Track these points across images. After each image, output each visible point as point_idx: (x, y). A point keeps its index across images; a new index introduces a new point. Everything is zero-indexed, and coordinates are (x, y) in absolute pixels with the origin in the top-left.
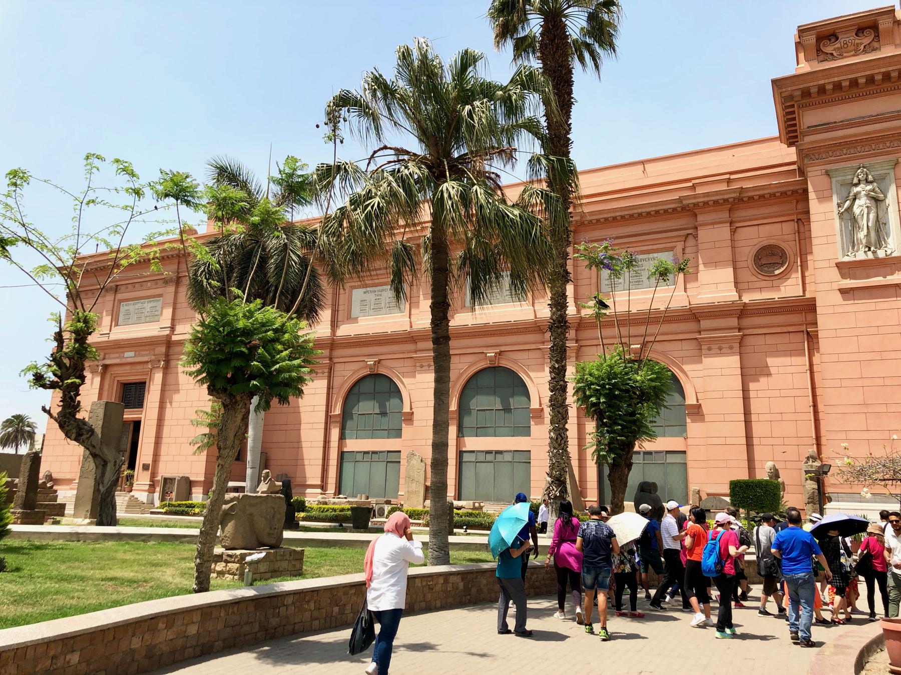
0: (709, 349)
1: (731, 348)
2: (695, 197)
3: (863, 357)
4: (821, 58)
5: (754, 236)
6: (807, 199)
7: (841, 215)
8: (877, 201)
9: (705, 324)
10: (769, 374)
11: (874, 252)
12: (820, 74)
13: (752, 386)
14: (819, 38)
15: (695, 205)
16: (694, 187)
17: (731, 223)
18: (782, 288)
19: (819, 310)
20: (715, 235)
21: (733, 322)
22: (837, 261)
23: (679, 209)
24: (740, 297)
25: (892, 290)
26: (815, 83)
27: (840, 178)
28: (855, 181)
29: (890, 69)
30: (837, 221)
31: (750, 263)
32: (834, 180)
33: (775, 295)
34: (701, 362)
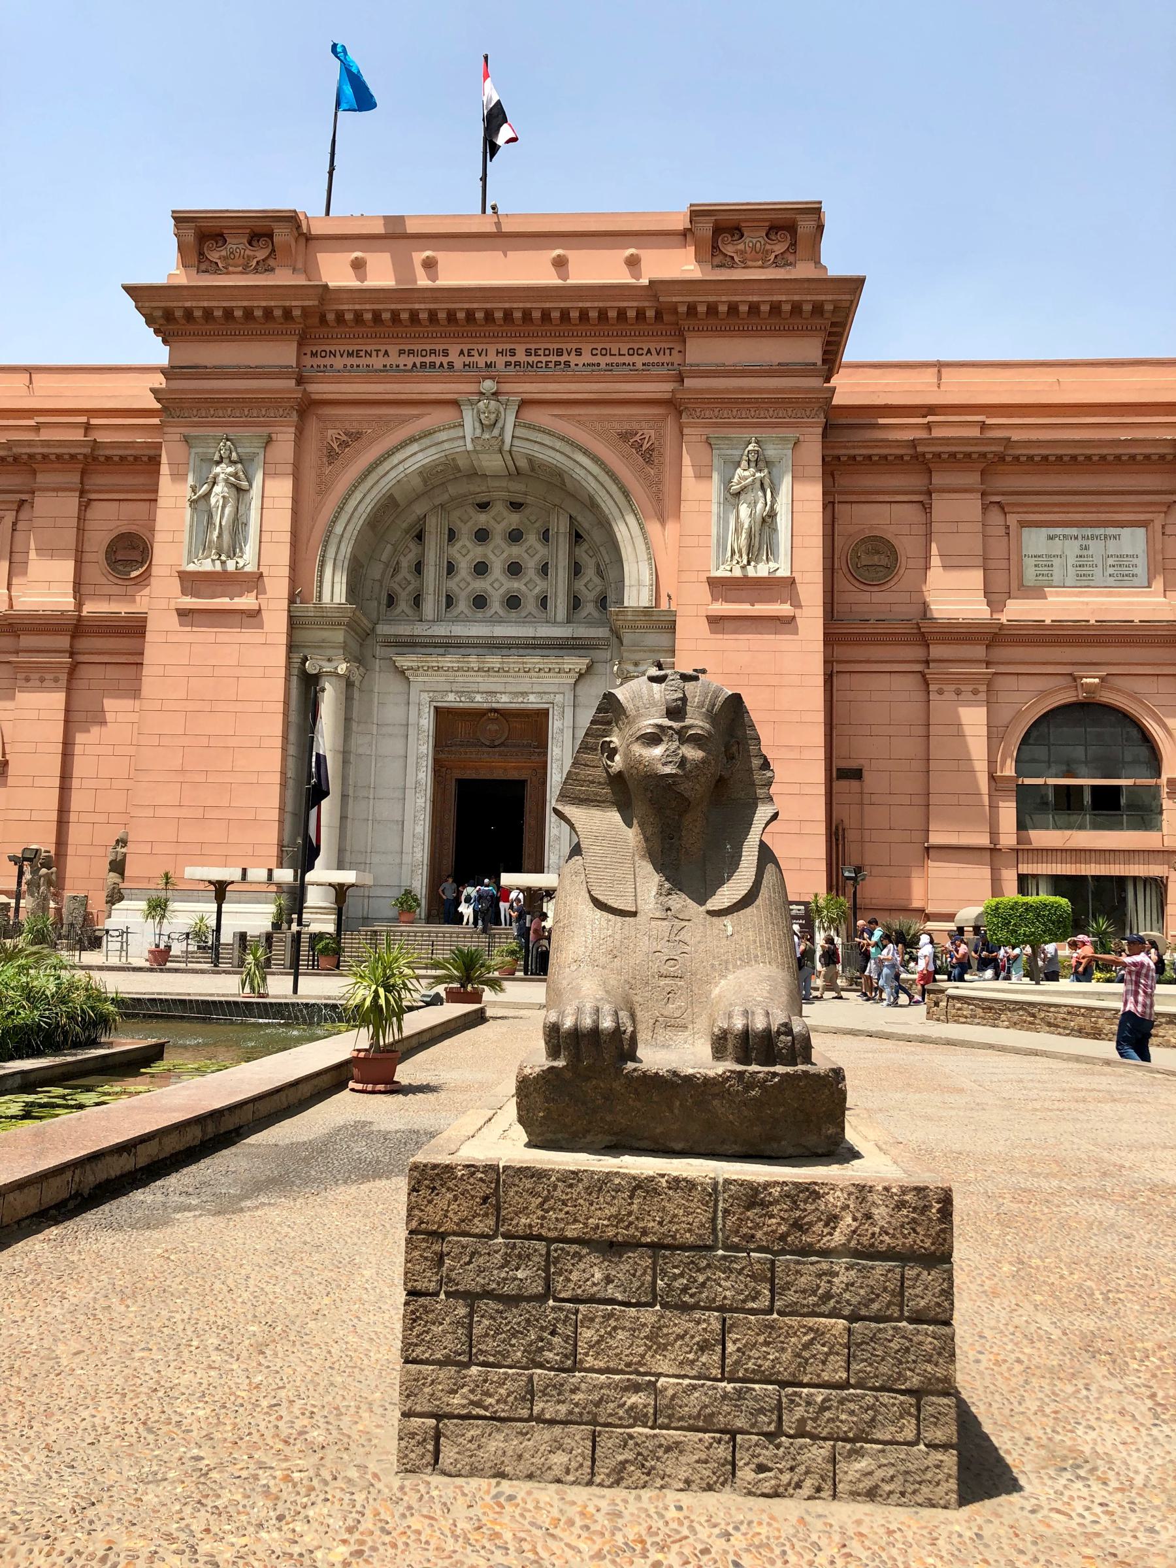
0: (27, 680)
1: (56, 680)
2: (30, 443)
3: (191, 706)
4: (203, 267)
5: (109, 519)
6: (158, 472)
7: (193, 502)
8: (240, 491)
9: (27, 641)
10: (103, 723)
11: (223, 563)
12: (185, 293)
13: (80, 738)
14: (202, 235)
15: (31, 456)
16: (37, 428)
17: (82, 493)
18: (138, 598)
19: (149, 637)
20: (56, 507)
21: (64, 642)
22: (182, 569)
23: (10, 459)
24: (79, 605)
25: (238, 617)
26: (180, 304)
27: (200, 450)
28: (216, 458)
29: (272, 303)
30: (188, 511)
31: (101, 557)
32: (193, 451)
33: (122, 608)
34: (13, 698)
